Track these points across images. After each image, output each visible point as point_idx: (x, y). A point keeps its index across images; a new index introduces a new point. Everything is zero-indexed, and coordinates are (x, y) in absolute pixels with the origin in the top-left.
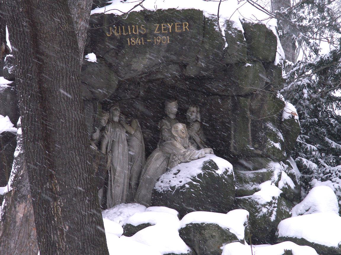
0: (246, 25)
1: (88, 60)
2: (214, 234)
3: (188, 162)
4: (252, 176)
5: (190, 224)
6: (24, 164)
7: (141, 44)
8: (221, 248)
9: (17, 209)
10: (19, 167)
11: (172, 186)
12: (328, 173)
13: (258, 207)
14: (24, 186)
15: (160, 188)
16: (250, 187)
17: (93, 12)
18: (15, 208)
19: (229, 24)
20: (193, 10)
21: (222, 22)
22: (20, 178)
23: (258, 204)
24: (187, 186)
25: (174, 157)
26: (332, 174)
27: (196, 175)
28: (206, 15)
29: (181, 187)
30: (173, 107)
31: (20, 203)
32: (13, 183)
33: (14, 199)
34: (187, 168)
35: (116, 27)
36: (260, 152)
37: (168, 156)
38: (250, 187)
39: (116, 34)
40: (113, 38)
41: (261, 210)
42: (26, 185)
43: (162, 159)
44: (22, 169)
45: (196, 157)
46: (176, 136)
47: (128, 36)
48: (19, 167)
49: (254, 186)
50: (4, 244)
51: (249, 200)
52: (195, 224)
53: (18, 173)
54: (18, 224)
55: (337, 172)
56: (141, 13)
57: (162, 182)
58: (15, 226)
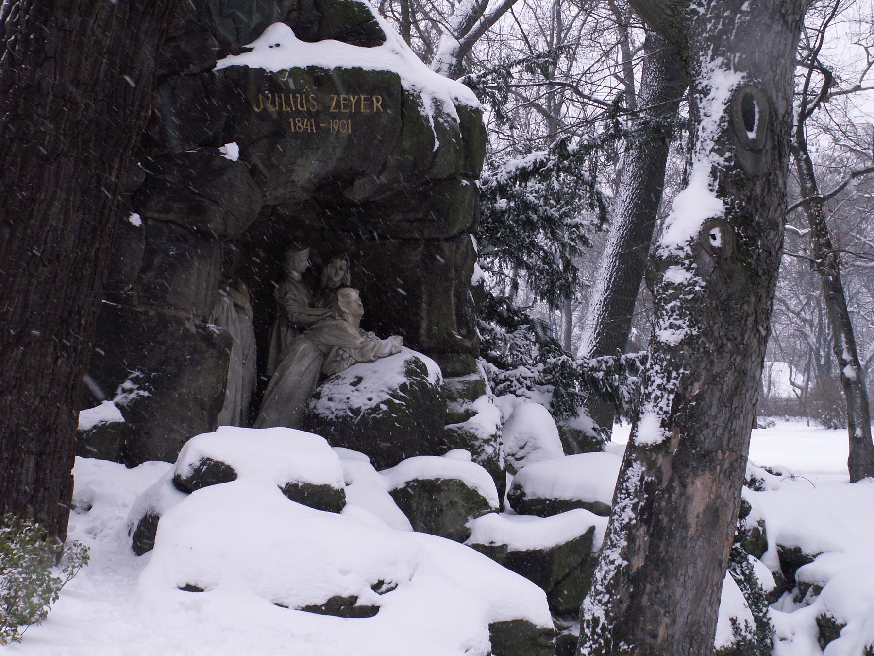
0: (460, 109)
1: (226, 157)
2: (456, 499)
3: (372, 361)
4: (460, 387)
5: (413, 481)
6: (703, 365)
7: (312, 130)
8: (467, 525)
9: (690, 490)
10: (688, 372)
11: (355, 406)
12: (504, 381)
13: (477, 443)
14: (707, 425)
15: (327, 412)
16: (459, 407)
17: (221, 64)
18: (684, 486)
19: (437, 104)
20: (389, 73)
21: (427, 101)
22: (694, 404)
23: (476, 438)
24: (384, 407)
25: (341, 352)
26: (512, 382)
27: (396, 386)
28: (406, 85)
29: (371, 409)
30: (301, 260)
31: (696, 475)
32: (670, 418)
33: (679, 464)
34: (374, 372)
35: (270, 95)
36: (468, 344)
37: (324, 350)
38: (459, 407)
39: (271, 109)
40: (264, 116)
41: (483, 450)
42: (711, 423)
43: (312, 355)
44: (698, 380)
45: (387, 351)
46: (347, 311)
47: (289, 115)
48: (688, 372)
49: (465, 406)
50: (655, 589)
51: (460, 432)
52: (423, 481)
53: (685, 389)
54: (692, 531)
55: (522, 380)
56: (307, 72)
57: (330, 399)
58: (684, 539)
